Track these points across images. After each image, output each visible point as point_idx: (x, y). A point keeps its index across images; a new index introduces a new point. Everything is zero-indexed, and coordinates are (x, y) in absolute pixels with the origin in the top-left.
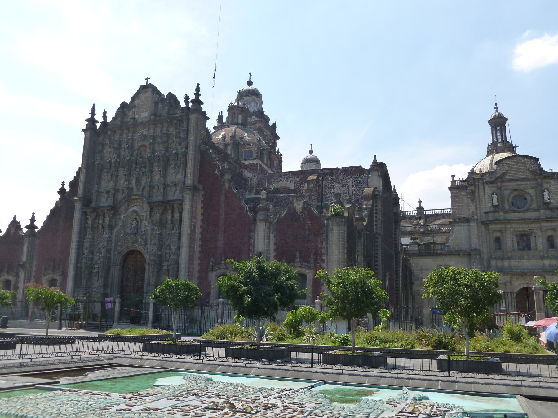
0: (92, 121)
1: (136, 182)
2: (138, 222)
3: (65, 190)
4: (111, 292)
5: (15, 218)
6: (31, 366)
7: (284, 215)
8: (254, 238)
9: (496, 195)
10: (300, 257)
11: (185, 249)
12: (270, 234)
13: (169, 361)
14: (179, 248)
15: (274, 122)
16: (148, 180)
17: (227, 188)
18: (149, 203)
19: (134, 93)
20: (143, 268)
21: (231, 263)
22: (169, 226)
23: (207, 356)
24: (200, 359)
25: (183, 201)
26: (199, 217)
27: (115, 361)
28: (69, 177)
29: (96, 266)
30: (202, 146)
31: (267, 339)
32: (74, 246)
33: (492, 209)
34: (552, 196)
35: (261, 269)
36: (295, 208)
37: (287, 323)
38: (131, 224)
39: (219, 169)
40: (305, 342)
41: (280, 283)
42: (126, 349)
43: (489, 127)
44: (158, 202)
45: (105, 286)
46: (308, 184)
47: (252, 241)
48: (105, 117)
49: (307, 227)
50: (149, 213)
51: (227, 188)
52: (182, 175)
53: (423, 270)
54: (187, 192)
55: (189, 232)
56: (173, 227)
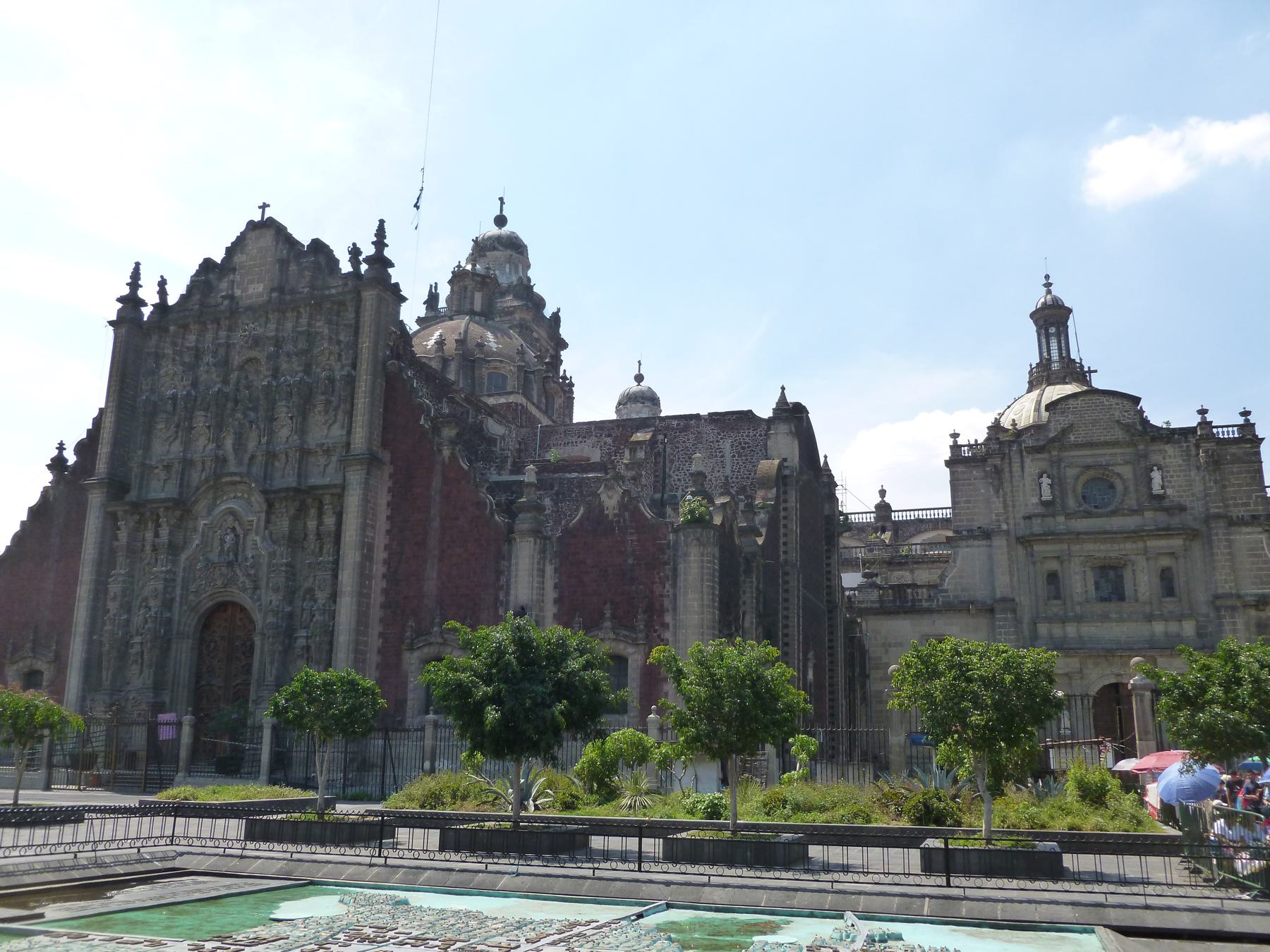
0: (131, 302)
1: (234, 445)
2: (237, 536)
3: (66, 461)
8: (509, 574)
9: (1048, 477)
10: (614, 617)
12: (544, 565)
13: (308, 861)
14: (334, 597)
16: (264, 440)
18: (264, 492)
19: (233, 239)
20: (248, 643)
21: (455, 630)
23: (397, 849)
24: (380, 856)
25: (343, 487)
26: (382, 524)
27: (177, 863)
28: (76, 431)
29: (137, 639)
31: (537, 808)
32: (83, 592)
33: (1040, 510)
35: (524, 645)
36: (603, 507)
37: (583, 768)
38: (222, 541)
39: (428, 415)
40: (625, 811)
41: (568, 677)
42: (206, 834)
43: (1032, 328)
44: (287, 489)
45: (158, 686)
46: (633, 451)
47: (503, 580)
48: (163, 293)
49: (630, 549)
50: (263, 516)
52: (343, 427)
53: (890, 645)
54: (354, 468)
55: (358, 559)
56: (321, 549)
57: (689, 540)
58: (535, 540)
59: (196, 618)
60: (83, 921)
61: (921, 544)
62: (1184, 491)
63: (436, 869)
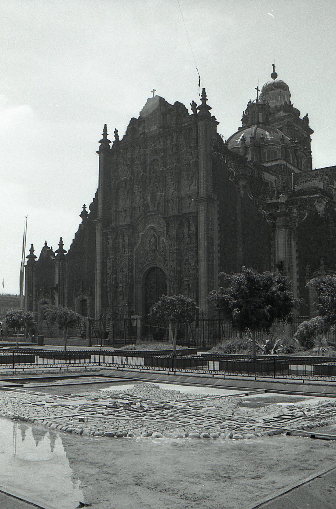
0: (104, 142)
3: (87, 212)
5: (46, 244)
6: (23, 374)
7: (306, 218)
8: (275, 247)
10: (325, 264)
11: (204, 263)
12: (291, 242)
13: (146, 373)
14: (197, 262)
17: (243, 196)
18: (164, 218)
21: (223, 276)
22: (187, 241)
23: (202, 370)
24: (173, 371)
25: (197, 213)
26: (216, 228)
28: (89, 200)
29: (120, 285)
30: (213, 154)
31: (275, 353)
32: (98, 266)
35: (251, 280)
36: (317, 211)
37: (298, 335)
39: (233, 175)
40: (314, 353)
41: (272, 294)
44: (174, 216)
45: (130, 304)
48: (116, 136)
50: (165, 228)
51: (243, 196)
52: (196, 186)
54: (201, 203)
56: (191, 241)
58: (285, 230)
60: (34, 388)
63: (193, 376)
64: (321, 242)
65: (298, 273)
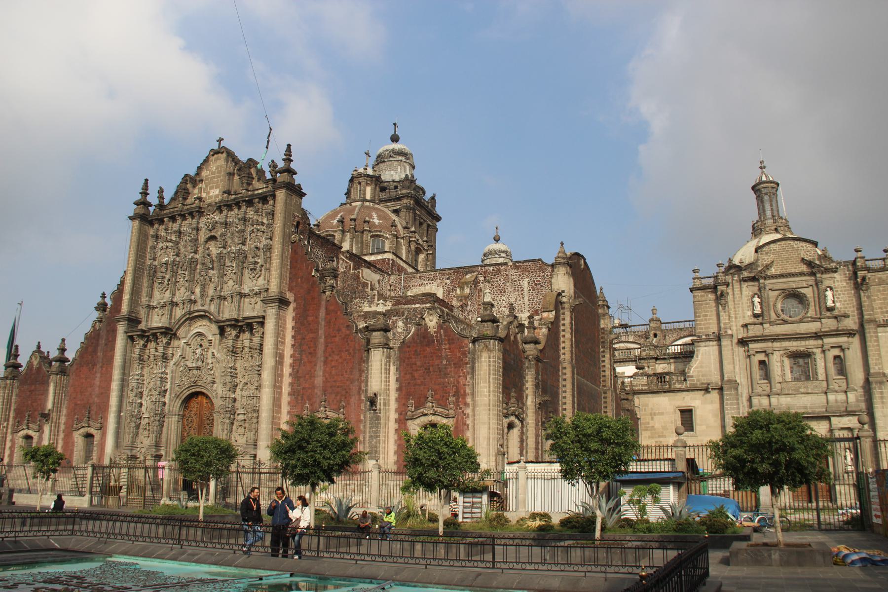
1: (201, 292)
4: (166, 453)
5: (39, 347)
7: (412, 335)
9: (758, 297)
15: (432, 195)
20: (211, 418)
26: (289, 340)
32: (115, 386)
33: (753, 320)
34: (838, 298)
45: (157, 445)
46: (462, 288)
47: (364, 375)
48: (161, 198)
49: (444, 354)
53: (655, 414)
55: (273, 364)
57: (481, 347)
59: (180, 403)
61: (680, 345)
62: (848, 304)
64: (429, 369)
65: (396, 410)
